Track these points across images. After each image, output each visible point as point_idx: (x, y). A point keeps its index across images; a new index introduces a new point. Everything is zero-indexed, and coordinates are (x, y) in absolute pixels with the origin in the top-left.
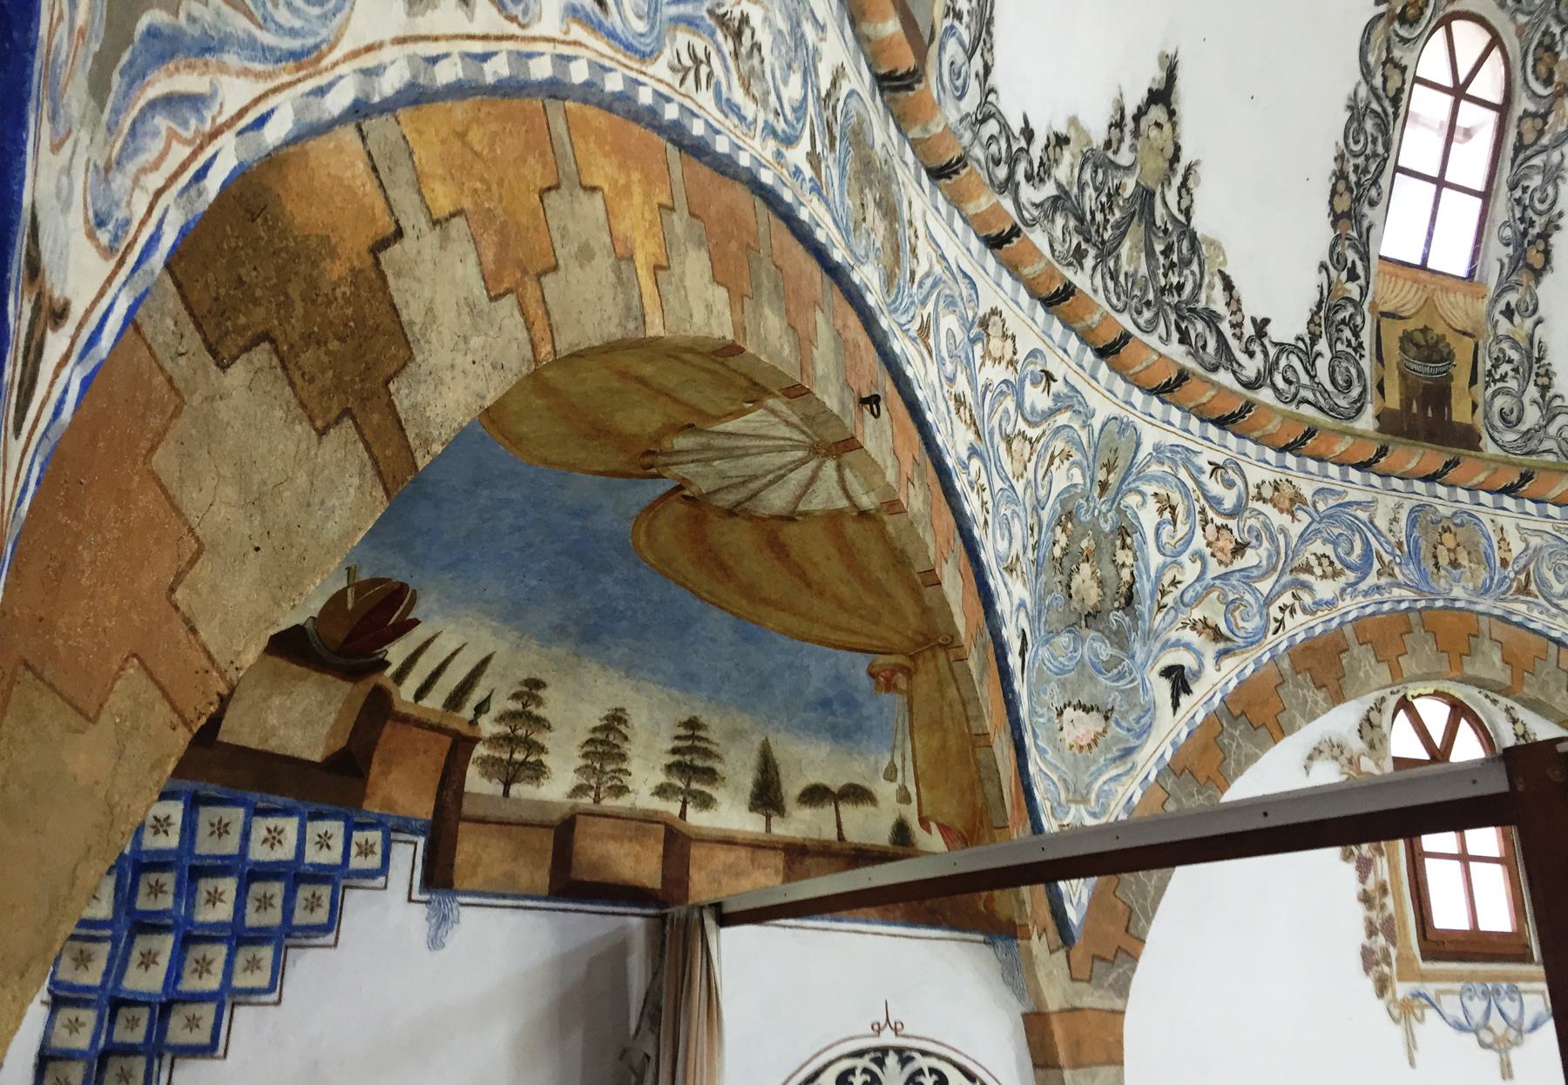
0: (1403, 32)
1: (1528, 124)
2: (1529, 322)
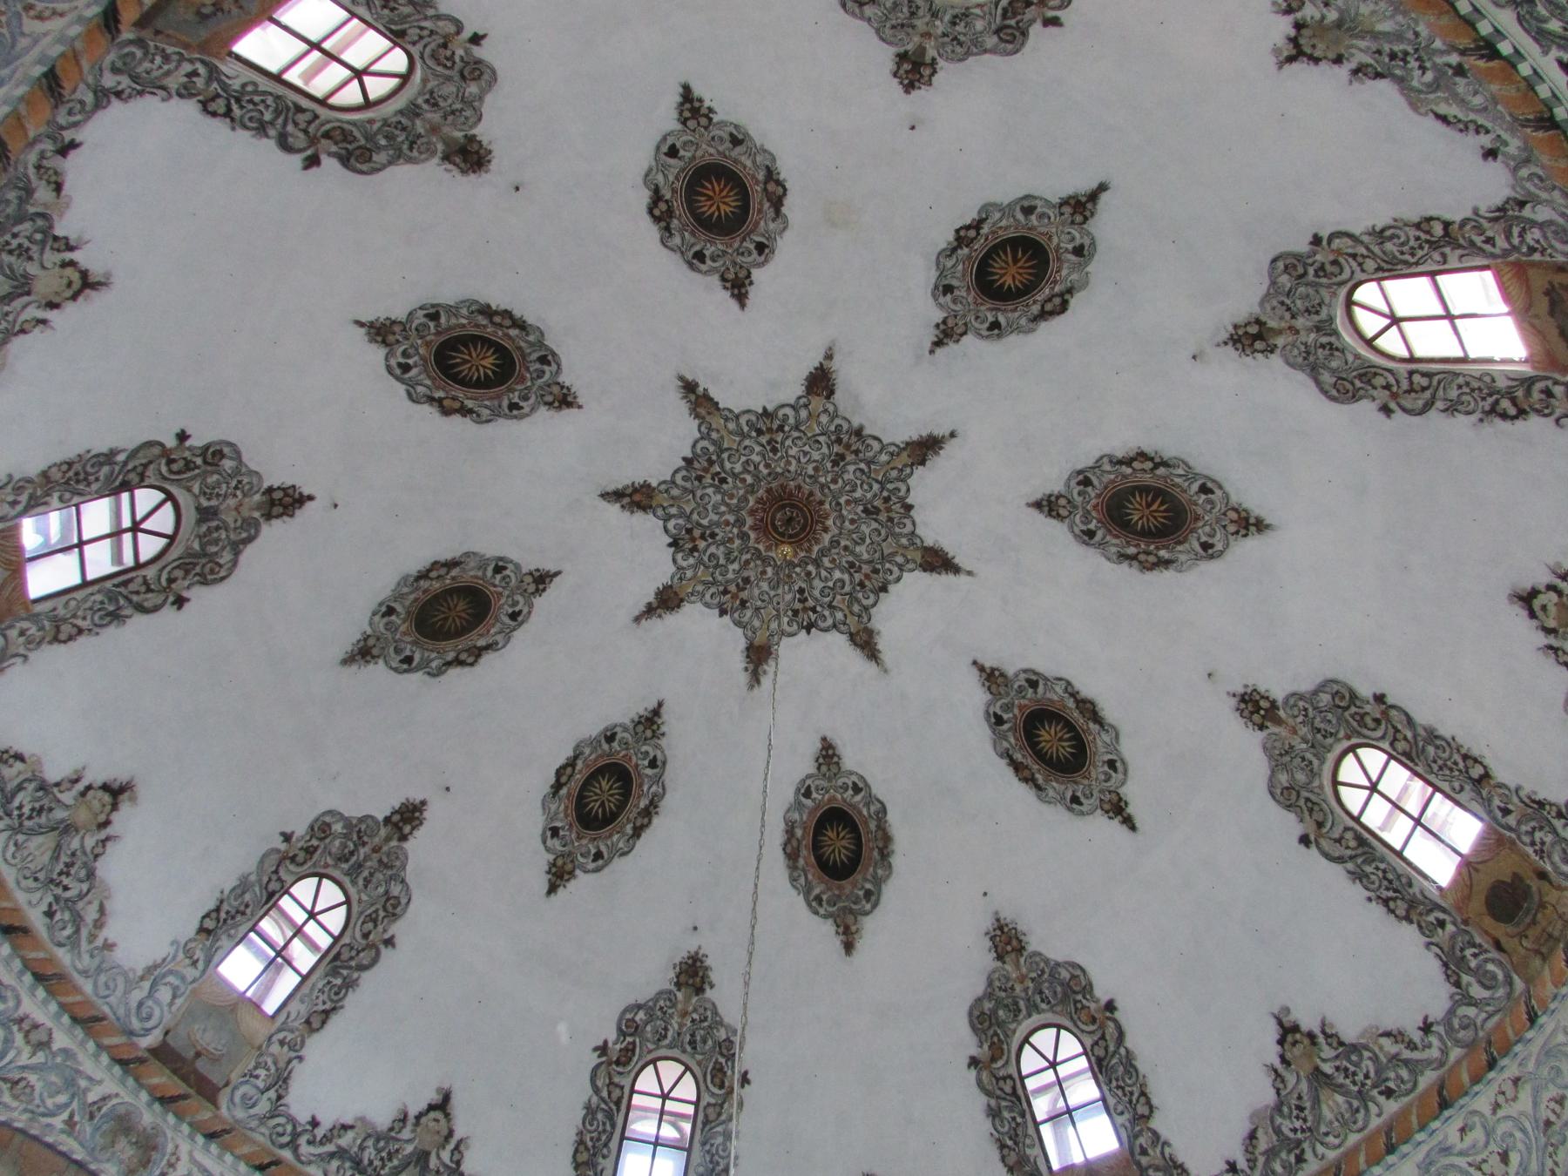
0: (620, 1069)
1: (710, 1110)
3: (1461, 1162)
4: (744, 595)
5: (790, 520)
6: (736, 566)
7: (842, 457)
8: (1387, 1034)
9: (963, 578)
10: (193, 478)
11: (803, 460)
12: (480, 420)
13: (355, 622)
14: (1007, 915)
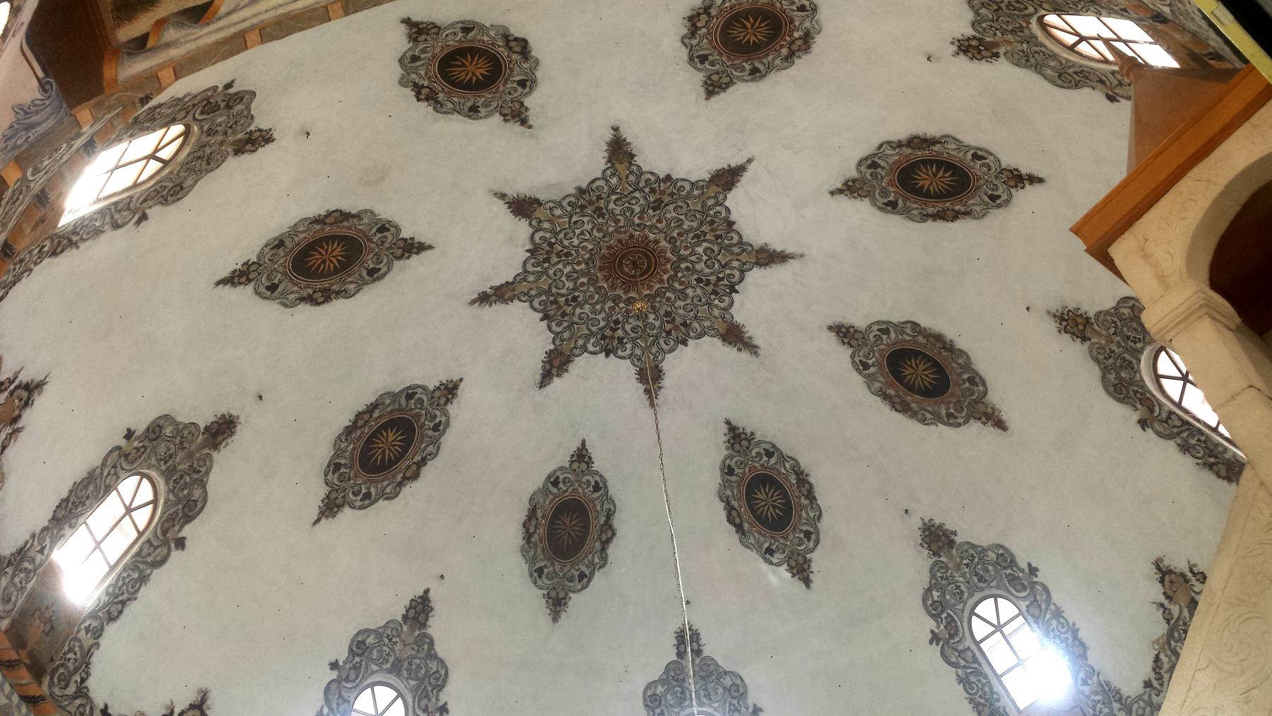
2: (1095, 678)
5: (634, 263)
6: (651, 317)
7: (599, 209)
9: (752, 168)
10: (367, 667)
11: (588, 236)
12: (434, 455)
13: (533, 598)
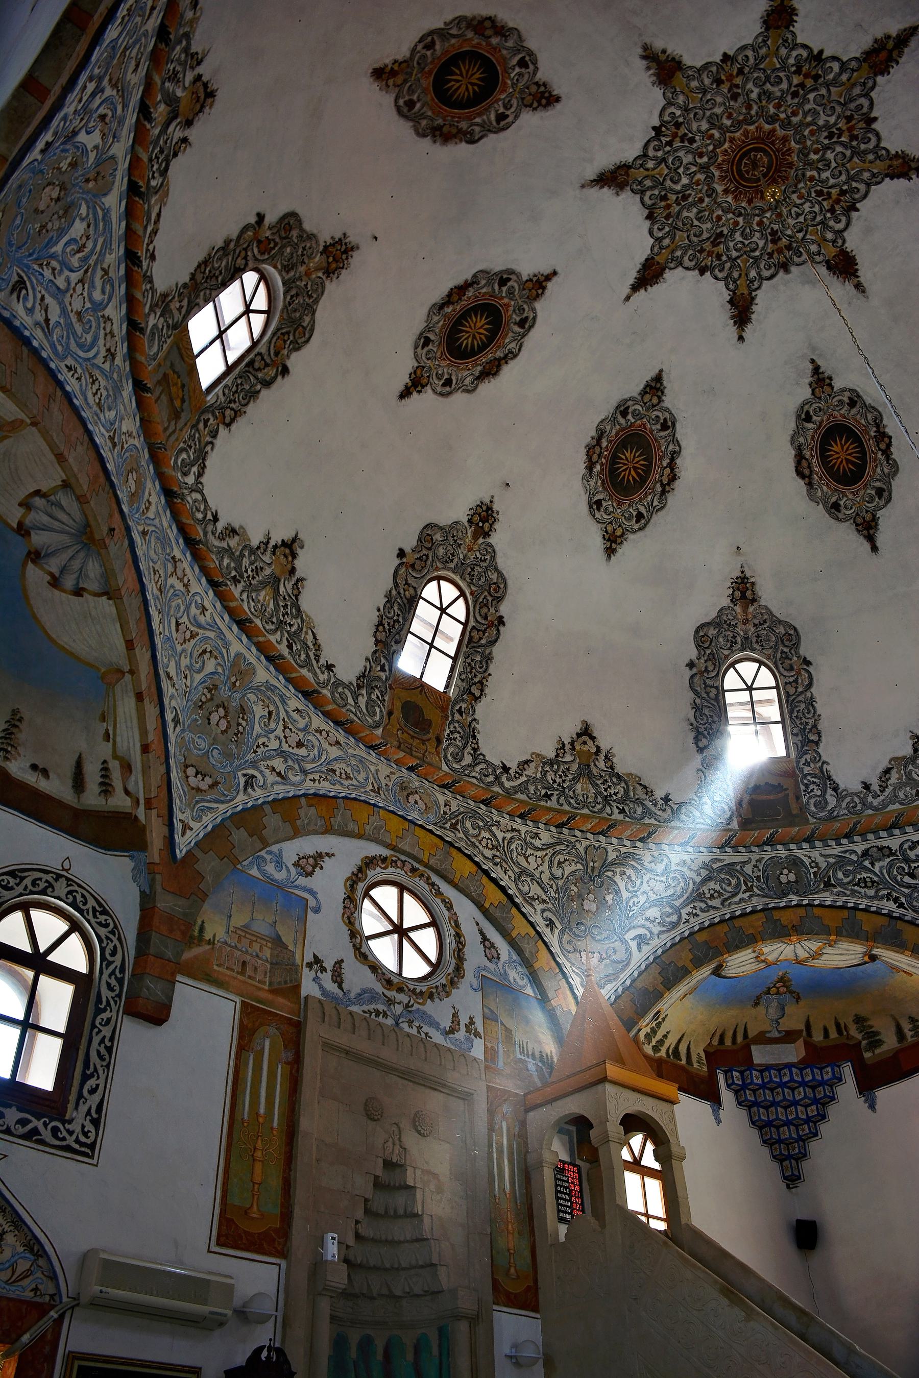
3: (283, 714)
4: (725, 88)
6: (754, 96)
7: (774, 242)
8: (315, 637)
9: (627, 290)
14: (356, 259)
